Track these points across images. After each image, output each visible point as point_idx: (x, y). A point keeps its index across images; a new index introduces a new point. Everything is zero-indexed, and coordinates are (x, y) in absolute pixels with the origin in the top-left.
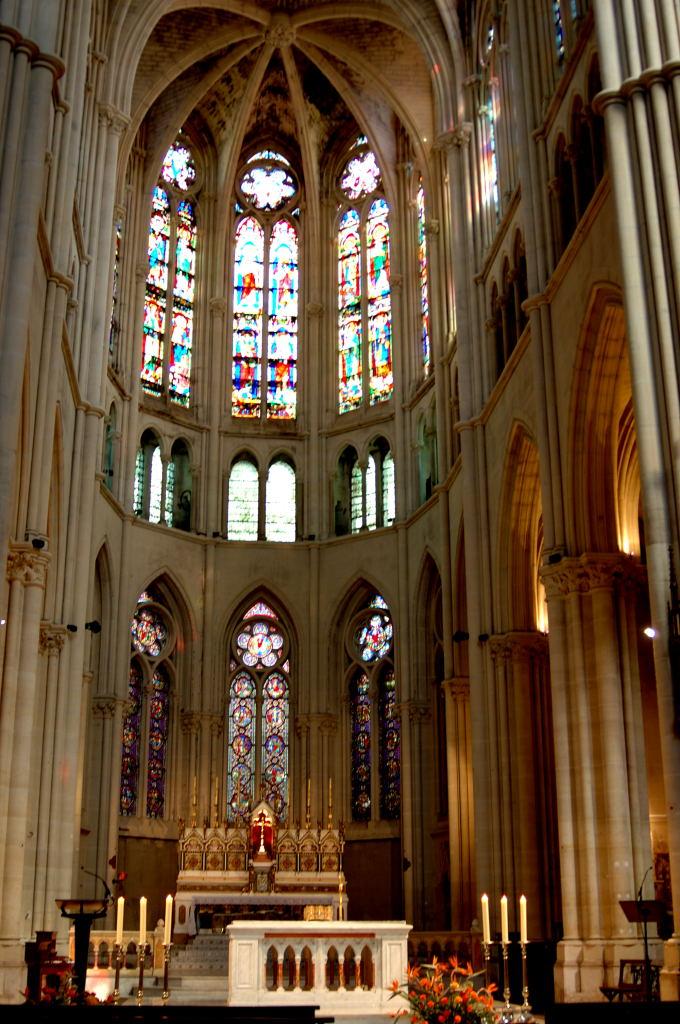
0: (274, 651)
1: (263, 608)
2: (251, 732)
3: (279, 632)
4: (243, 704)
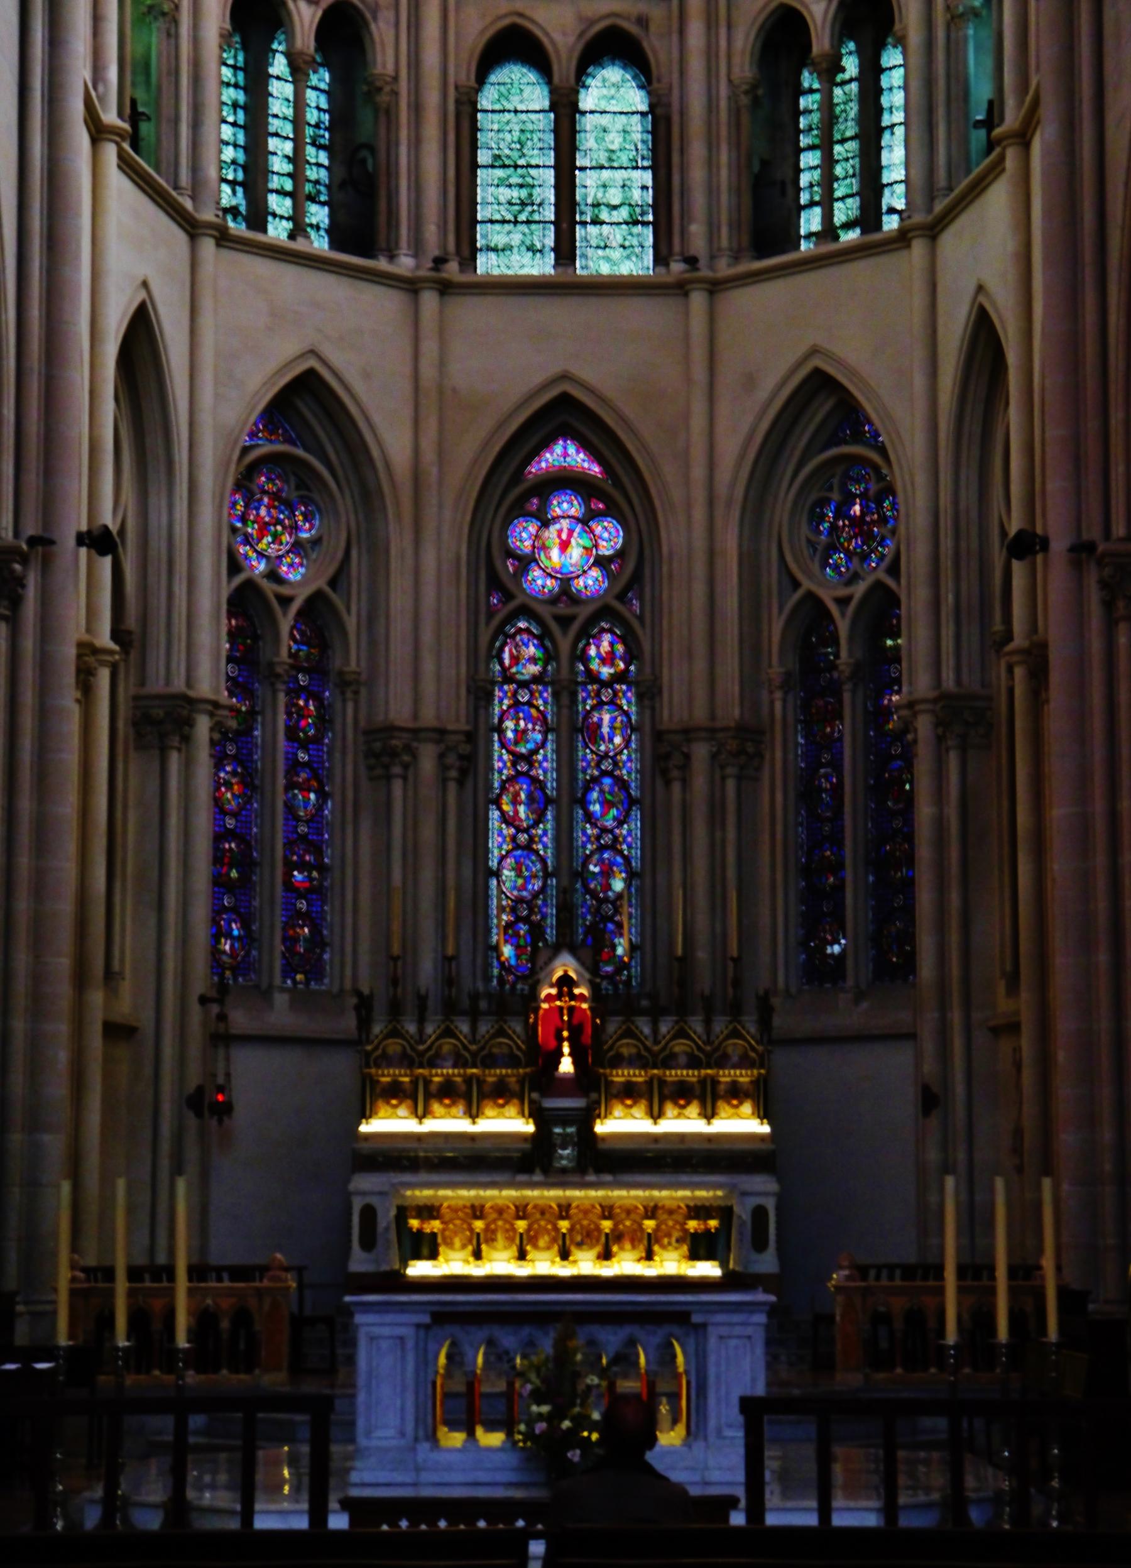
0: (601, 562)
1: (572, 450)
2: (546, 767)
3: (612, 511)
4: (524, 697)
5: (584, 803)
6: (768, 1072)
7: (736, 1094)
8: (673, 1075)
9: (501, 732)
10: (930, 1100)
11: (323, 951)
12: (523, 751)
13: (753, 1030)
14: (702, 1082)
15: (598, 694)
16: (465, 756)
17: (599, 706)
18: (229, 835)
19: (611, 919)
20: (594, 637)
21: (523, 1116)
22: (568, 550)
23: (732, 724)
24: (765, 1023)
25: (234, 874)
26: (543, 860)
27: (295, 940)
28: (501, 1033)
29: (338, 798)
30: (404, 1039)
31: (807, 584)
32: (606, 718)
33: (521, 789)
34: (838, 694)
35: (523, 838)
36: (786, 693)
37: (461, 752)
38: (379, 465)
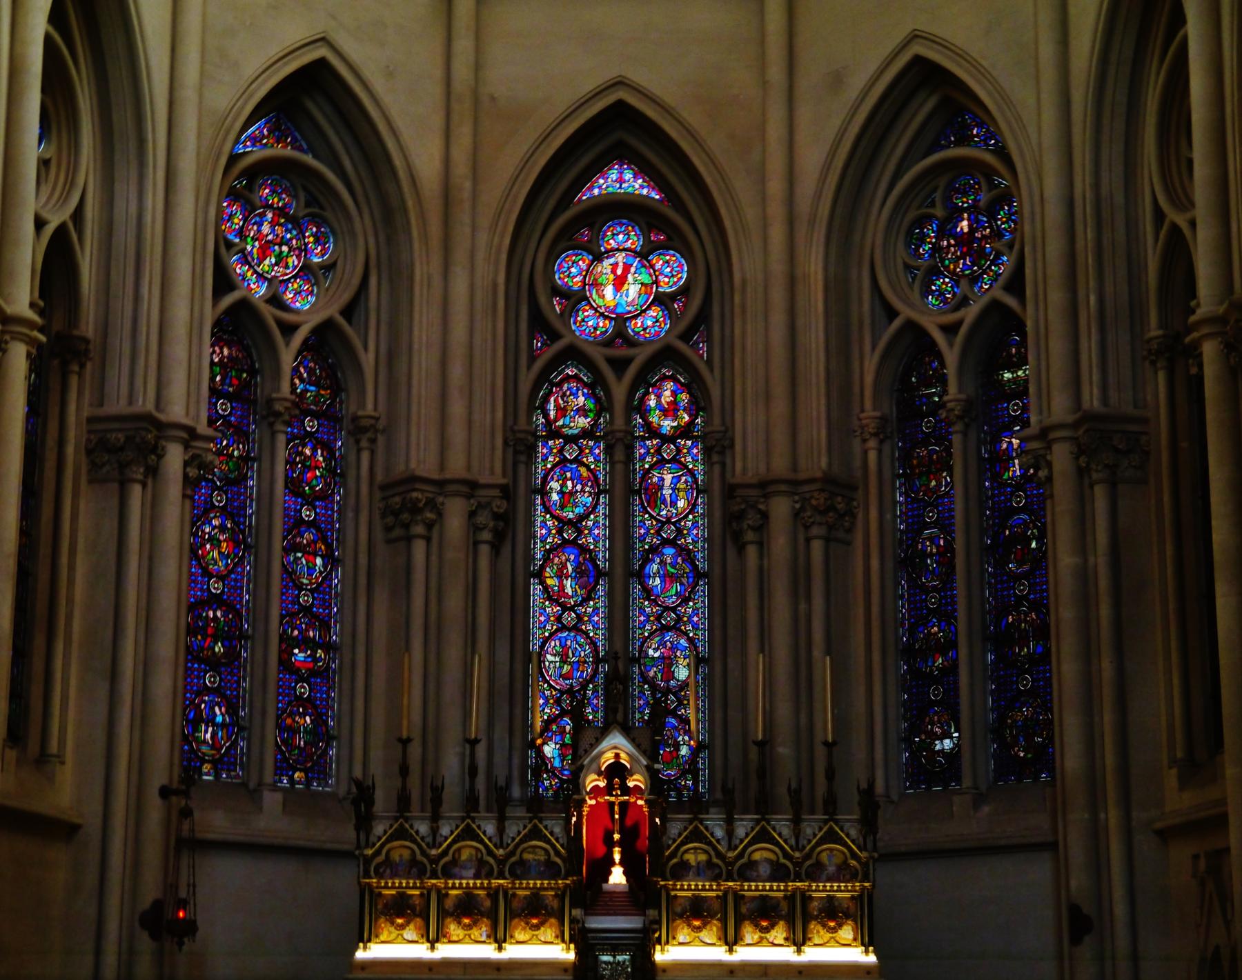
0: (661, 300)
1: (628, 175)
2: (596, 534)
4: (571, 453)
5: (641, 576)
6: (873, 886)
7: (832, 914)
8: (753, 889)
9: (544, 492)
10: (1079, 924)
11: (329, 745)
12: (571, 516)
13: (853, 833)
14: (790, 898)
15: (658, 451)
16: (502, 517)
17: (661, 463)
18: (215, 601)
19: (673, 713)
20: (654, 385)
21: (563, 941)
22: (622, 287)
23: (819, 474)
24: (869, 824)
25: (219, 648)
26: (593, 643)
27: (294, 731)
28: (535, 834)
29: (349, 562)
30: (414, 841)
31: (906, 312)
32: (668, 478)
33: (568, 560)
34: (943, 438)
35: (570, 618)
36: (881, 442)
37: (495, 510)
38: (402, 174)
